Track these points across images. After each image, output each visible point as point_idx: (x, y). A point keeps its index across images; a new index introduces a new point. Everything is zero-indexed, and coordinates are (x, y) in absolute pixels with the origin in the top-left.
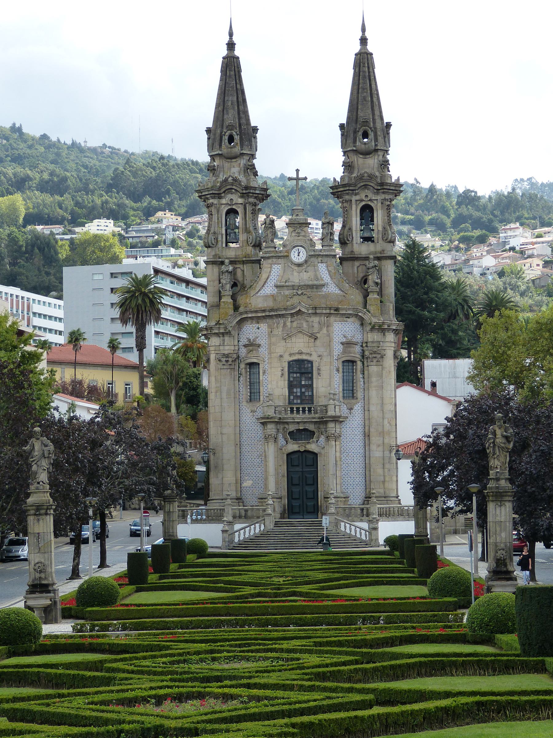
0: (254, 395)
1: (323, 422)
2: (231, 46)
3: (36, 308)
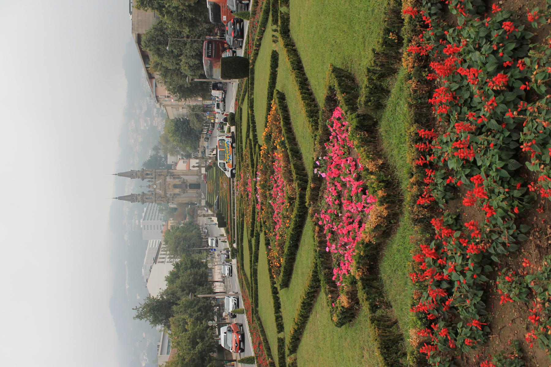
0: (179, 194)
1: (185, 183)
2: (116, 198)
3: (151, 247)
